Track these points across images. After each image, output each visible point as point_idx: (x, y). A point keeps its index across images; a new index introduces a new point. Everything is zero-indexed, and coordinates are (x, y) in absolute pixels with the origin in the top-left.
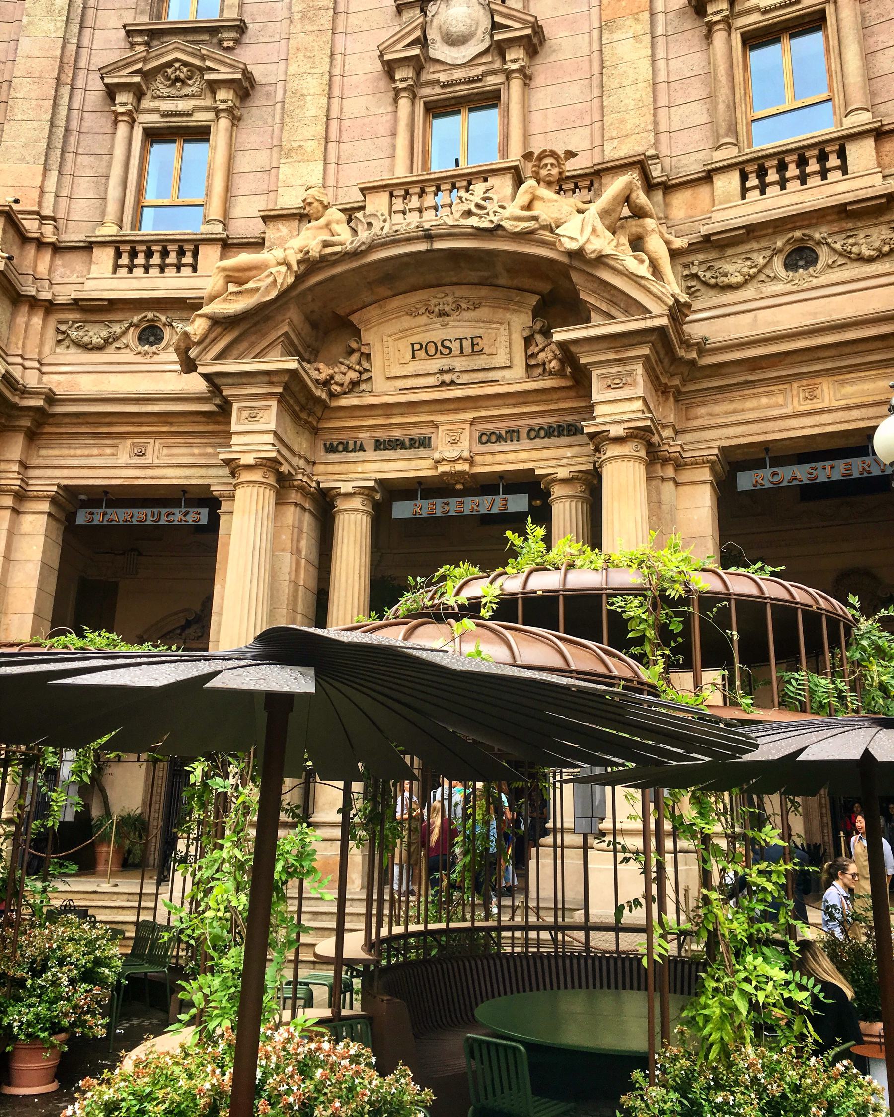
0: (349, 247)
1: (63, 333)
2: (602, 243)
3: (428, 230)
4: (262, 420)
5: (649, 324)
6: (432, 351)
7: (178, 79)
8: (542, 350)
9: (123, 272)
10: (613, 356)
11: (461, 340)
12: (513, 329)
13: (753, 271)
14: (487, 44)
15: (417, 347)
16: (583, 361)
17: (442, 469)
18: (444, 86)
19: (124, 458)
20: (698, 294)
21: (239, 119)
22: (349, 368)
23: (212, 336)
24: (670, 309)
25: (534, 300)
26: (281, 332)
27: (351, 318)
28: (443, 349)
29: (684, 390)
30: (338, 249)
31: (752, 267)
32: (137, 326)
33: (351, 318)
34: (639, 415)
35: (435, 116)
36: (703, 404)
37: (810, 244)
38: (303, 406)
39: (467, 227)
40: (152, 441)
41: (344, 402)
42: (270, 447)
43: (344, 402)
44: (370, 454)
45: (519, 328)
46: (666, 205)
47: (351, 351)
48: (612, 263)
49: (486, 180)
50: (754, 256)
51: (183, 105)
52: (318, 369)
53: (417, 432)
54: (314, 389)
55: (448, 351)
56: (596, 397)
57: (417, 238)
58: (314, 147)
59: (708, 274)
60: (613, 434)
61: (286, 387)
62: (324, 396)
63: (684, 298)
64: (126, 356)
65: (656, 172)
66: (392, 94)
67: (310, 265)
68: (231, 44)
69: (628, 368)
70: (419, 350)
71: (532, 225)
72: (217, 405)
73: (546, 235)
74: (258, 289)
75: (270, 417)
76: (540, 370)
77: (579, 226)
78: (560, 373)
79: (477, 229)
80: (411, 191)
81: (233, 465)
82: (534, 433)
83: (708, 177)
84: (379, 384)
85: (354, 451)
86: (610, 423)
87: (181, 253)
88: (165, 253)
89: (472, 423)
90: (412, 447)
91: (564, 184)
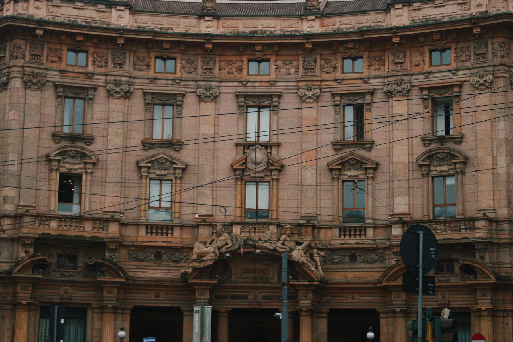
1: (131, 254)
9: (149, 235)
17: (251, 307)
41: (223, 285)
43: (223, 285)
46: (319, 233)
51: (163, 172)
59: (329, 258)
84: (234, 279)
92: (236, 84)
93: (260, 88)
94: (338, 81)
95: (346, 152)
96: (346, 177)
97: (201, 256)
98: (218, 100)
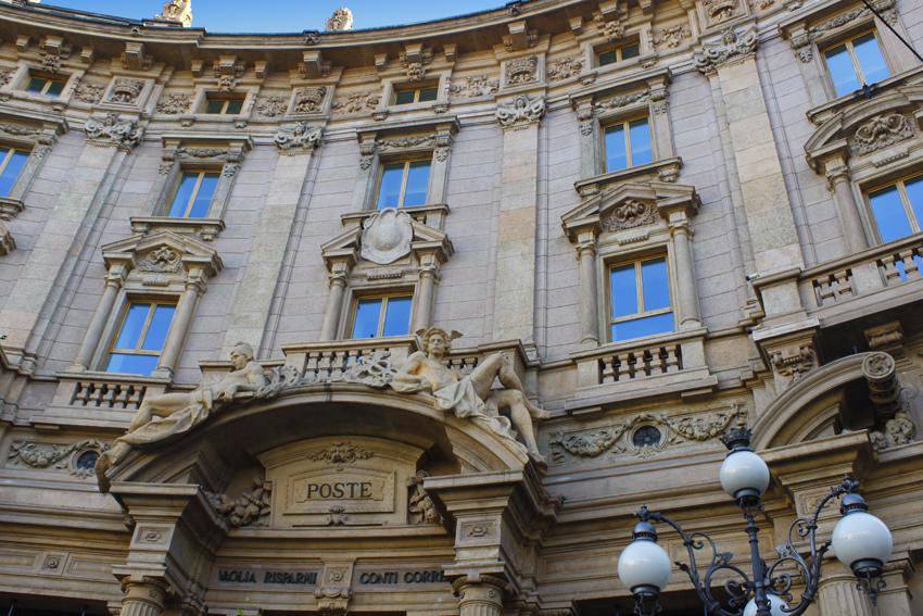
0: (259, 394)
1: (16, 450)
2: (474, 404)
3: (329, 385)
4: (160, 541)
5: (507, 478)
6: (326, 493)
7: (162, 259)
8: (422, 499)
9: (79, 403)
10: (476, 506)
11: (353, 484)
12: (399, 479)
13: (607, 443)
14: (408, 251)
15: (313, 488)
16: (449, 508)
18: (370, 279)
19: (37, 569)
20: (562, 460)
21: (204, 292)
22: (251, 502)
23: (128, 460)
24: (526, 466)
25: (418, 454)
26: (193, 462)
27: (258, 457)
28: (335, 492)
29: (544, 545)
30: (250, 394)
31: (605, 440)
32: (79, 450)
33: (258, 457)
34: (496, 561)
35: (362, 302)
36: (559, 560)
37: (654, 424)
39: (362, 384)
40: (66, 554)
41: (242, 533)
42: (160, 567)
43: (242, 533)
44: (260, 585)
45: (405, 477)
46: (539, 384)
47: (256, 487)
48: (479, 423)
49: (387, 349)
50: (610, 431)
51: (160, 278)
52: (221, 500)
53: (306, 568)
54: (213, 517)
55: (340, 494)
56: (458, 542)
57: (319, 391)
58: (259, 318)
59: (571, 444)
60: (470, 578)
61: (186, 512)
62: (223, 525)
63: (540, 458)
64: (64, 476)
65: (531, 356)
66: (328, 282)
67: (223, 406)
68: (210, 237)
69: (489, 518)
71: (414, 386)
72: (127, 526)
73: (426, 396)
74: (175, 422)
76: (419, 518)
77: (449, 391)
78: (436, 521)
79: (369, 386)
80: (324, 354)
81: (124, 581)
82: (411, 577)
83: (574, 363)
85: (245, 581)
86: (467, 568)
87: (131, 392)
88: (118, 391)
89: (356, 562)
90: (298, 581)
91: (446, 356)
94: (586, 81)
96: (616, 247)
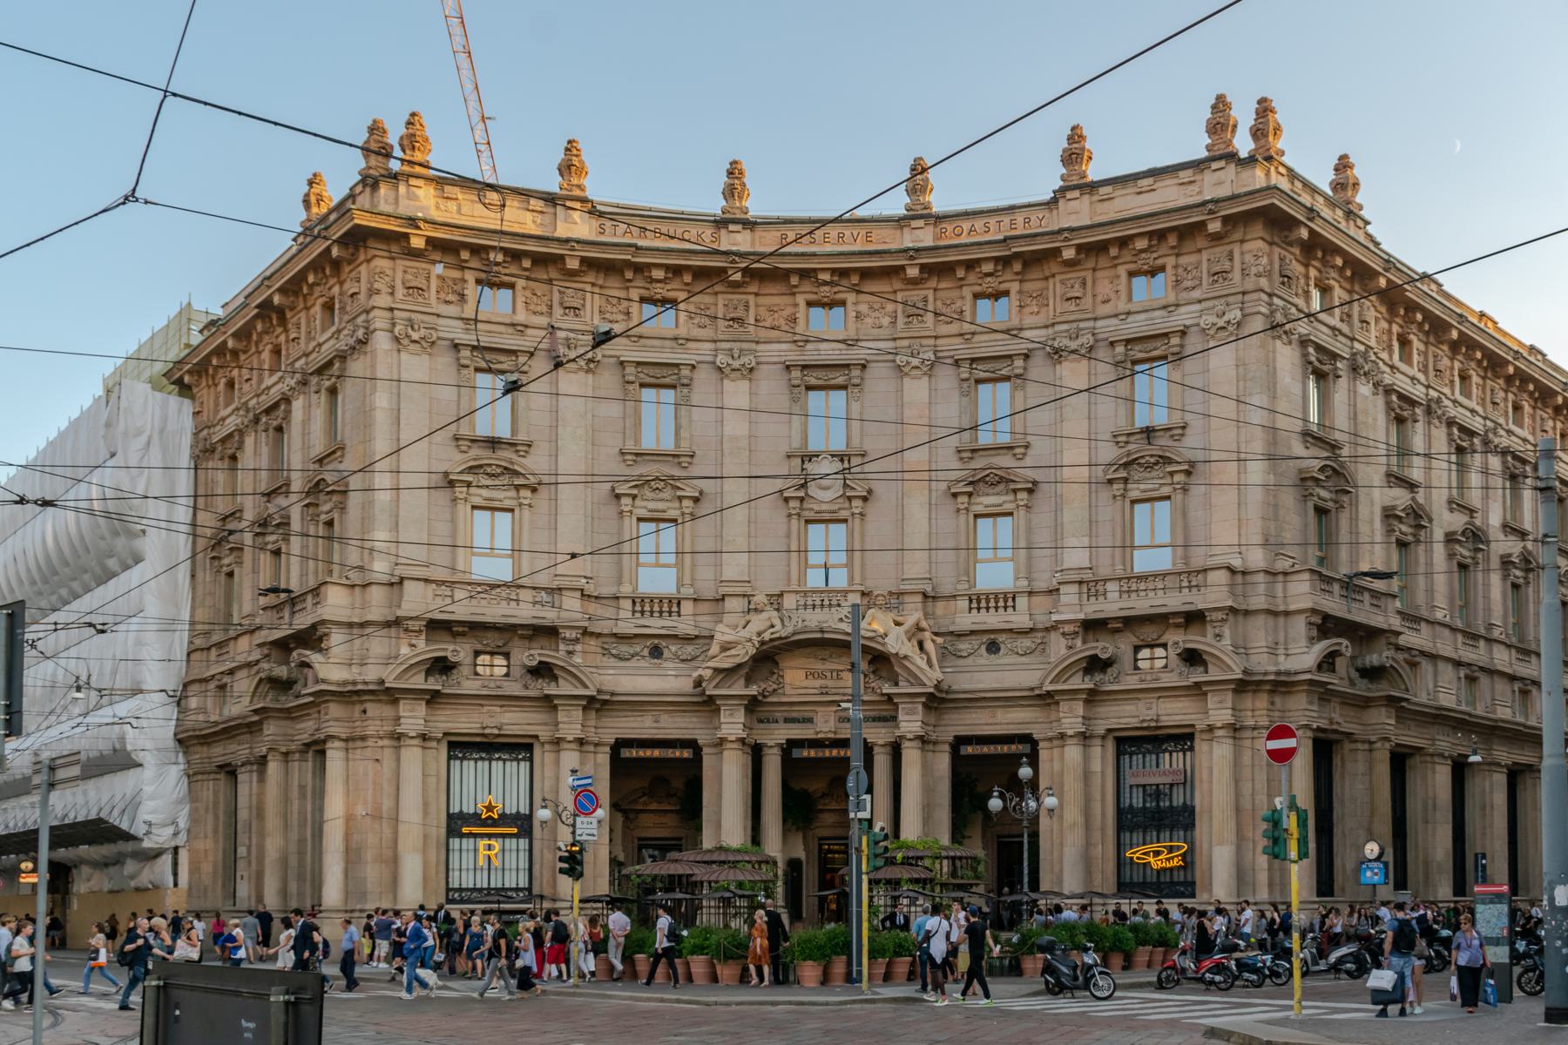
38: (753, 705)
44: (781, 725)
51: (660, 505)
53: (807, 715)
64: (643, 663)
70: (811, 674)
75: (740, 716)
84: (788, 690)
92: (784, 346)
93: (829, 353)
95: (979, 463)
97: (725, 648)
98: (755, 374)
